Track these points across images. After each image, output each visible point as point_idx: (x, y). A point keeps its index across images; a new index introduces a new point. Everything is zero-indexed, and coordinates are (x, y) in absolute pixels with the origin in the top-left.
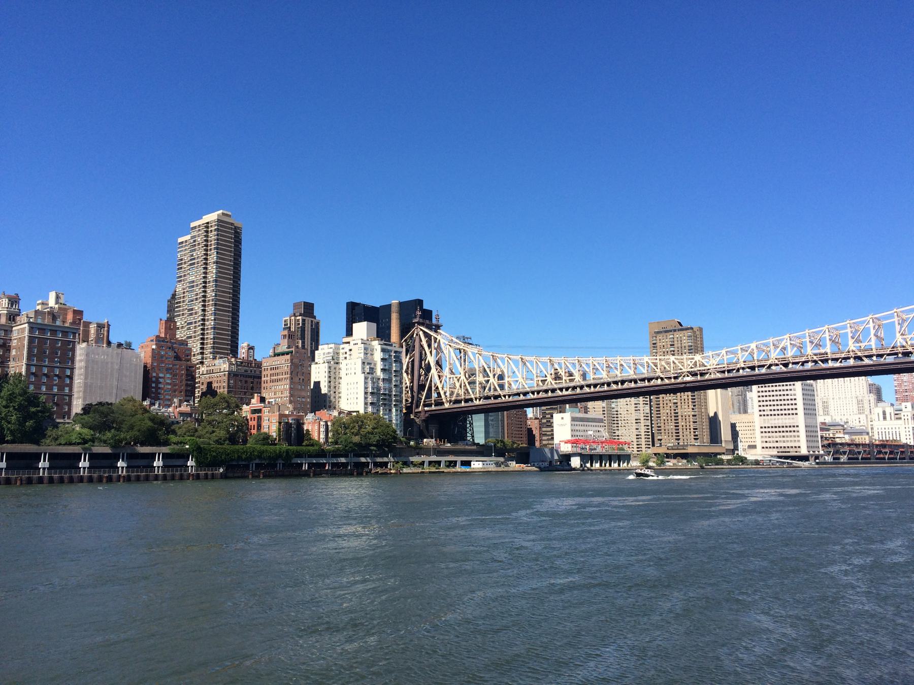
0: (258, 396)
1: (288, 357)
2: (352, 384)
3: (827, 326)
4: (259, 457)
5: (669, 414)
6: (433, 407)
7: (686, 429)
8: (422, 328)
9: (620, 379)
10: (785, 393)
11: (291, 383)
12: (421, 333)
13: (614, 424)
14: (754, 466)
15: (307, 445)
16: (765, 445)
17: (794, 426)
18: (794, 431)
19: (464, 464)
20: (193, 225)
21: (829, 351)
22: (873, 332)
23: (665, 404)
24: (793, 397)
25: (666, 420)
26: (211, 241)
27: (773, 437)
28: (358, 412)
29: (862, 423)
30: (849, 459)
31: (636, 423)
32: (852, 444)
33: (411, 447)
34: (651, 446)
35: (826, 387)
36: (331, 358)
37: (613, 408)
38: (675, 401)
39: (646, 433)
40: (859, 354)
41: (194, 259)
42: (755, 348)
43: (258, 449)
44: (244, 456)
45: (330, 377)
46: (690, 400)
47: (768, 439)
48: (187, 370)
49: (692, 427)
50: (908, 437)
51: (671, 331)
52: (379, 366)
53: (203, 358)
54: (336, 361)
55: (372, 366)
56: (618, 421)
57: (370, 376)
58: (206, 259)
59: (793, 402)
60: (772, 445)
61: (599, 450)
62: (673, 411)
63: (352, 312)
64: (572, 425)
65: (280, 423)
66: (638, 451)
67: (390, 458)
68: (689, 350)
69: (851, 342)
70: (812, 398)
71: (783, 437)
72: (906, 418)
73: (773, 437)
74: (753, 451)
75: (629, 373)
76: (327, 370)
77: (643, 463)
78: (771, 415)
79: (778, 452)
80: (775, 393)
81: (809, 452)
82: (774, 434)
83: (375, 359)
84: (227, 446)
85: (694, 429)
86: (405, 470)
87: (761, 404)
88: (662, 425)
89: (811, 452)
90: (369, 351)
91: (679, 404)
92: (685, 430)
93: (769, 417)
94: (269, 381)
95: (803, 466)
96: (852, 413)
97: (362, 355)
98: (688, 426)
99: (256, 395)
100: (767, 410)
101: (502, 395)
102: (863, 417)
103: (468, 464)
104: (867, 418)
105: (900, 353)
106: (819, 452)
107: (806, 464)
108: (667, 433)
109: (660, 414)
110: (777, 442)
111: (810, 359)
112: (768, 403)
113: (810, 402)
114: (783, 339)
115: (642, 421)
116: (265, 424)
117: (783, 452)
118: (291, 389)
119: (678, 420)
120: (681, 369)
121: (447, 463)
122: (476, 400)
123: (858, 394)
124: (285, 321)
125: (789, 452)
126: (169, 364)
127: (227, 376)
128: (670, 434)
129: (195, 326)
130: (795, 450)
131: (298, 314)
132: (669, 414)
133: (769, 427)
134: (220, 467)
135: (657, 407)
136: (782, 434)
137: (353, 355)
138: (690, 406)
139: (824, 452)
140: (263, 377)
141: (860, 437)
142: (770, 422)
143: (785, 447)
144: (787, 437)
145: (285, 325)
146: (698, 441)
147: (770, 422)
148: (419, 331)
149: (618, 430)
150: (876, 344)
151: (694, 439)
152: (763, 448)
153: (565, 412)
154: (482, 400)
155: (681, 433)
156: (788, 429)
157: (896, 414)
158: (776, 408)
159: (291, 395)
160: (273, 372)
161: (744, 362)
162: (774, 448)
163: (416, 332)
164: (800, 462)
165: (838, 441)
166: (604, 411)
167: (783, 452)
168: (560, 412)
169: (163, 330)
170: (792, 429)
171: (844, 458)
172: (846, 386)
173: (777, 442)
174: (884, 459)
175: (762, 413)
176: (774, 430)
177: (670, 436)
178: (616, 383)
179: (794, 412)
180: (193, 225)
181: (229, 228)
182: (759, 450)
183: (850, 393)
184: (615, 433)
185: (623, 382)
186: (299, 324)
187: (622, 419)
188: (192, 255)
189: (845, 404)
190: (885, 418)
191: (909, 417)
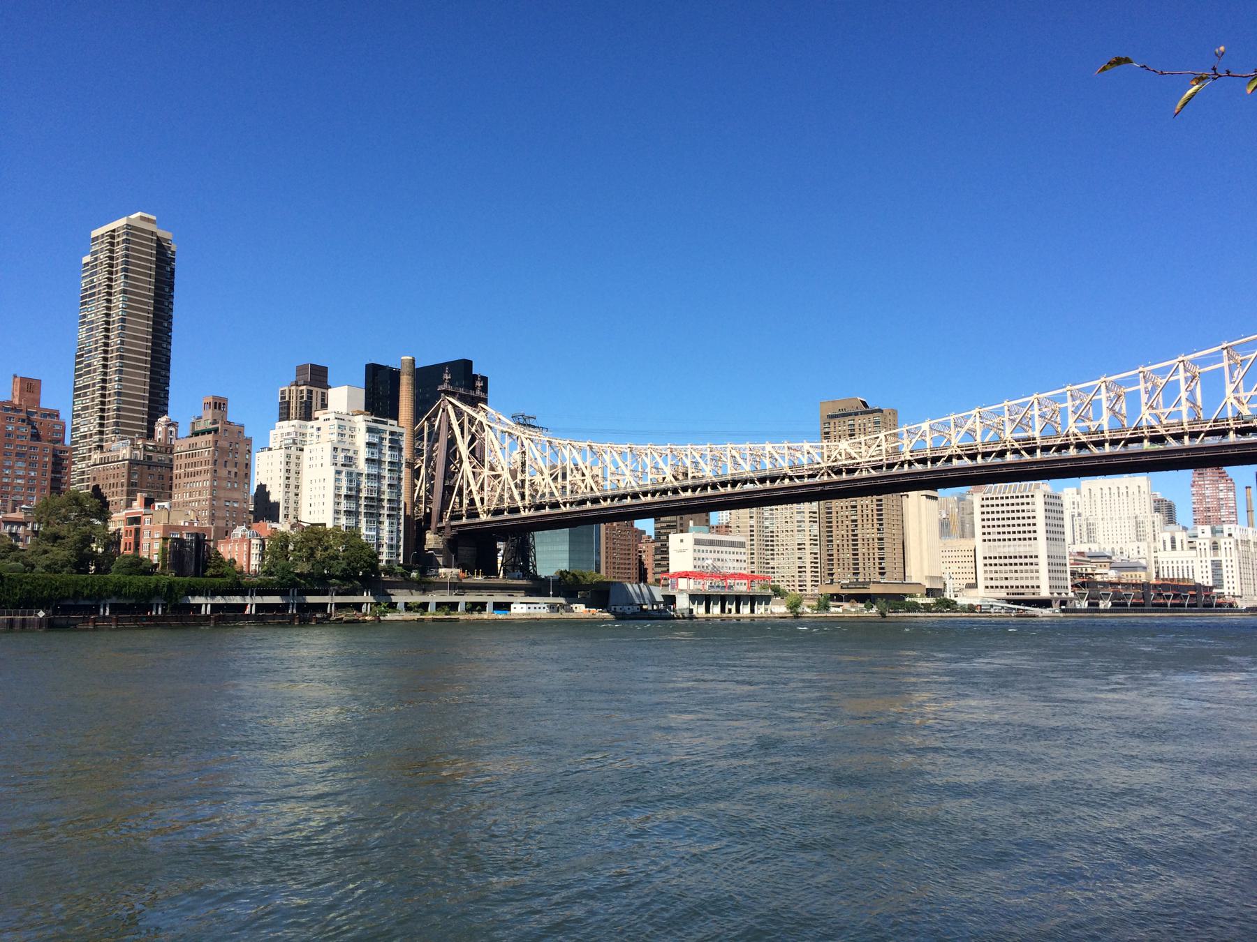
0: (142, 496)
1: (210, 437)
2: (318, 481)
3: (1035, 396)
4: (117, 593)
5: (845, 536)
6: (464, 521)
7: (869, 559)
8: (451, 399)
9: (729, 478)
10: (1020, 508)
11: (214, 479)
12: (450, 407)
13: (768, 550)
14: (964, 614)
15: (212, 576)
17: (1031, 557)
18: (1031, 564)
19: (498, 606)
20: (94, 234)
21: (1037, 434)
22: (1105, 404)
23: (840, 522)
24: (1031, 514)
25: (841, 546)
26: (118, 259)
27: (1001, 572)
28: (325, 525)
29: (1142, 554)
30: (1113, 605)
31: (799, 549)
32: (1118, 584)
33: (413, 580)
34: (819, 583)
35: (1093, 503)
36: (291, 441)
37: (767, 527)
38: (854, 518)
39: (813, 565)
40: (1084, 439)
41: (94, 287)
42: (928, 430)
43: (114, 580)
44: (86, 592)
45: (288, 471)
46: (875, 517)
47: (993, 575)
48: (55, 456)
49: (877, 555)
50: (1205, 575)
51: (850, 414)
52: (363, 453)
53: (101, 440)
54: (299, 446)
55: (351, 454)
56: (773, 546)
57: (344, 469)
58: (110, 287)
59: (1031, 521)
60: (999, 583)
61: (741, 588)
62: (850, 533)
63: (373, 379)
64: (695, 550)
65: (165, 539)
66: (800, 590)
67: (366, 598)
69: (1071, 420)
70: (1059, 515)
71: (1016, 571)
72: (1203, 547)
73: (1001, 572)
74: (972, 592)
75: (743, 468)
76: (283, 459)
77: (791, 608)
78: (999, 540)
79: (1008, 594)
80: (1005, 508)
81: (1051, 593)
82: (1003, 568)
83: (357, 444)
84: (67, 575)
85: (880, 559)
86: (389, 617)
87: (986, 523)
88: (835, 552)
89: (1056, 595)
90: (347, 432)
91: (859, 522)
92: (867, 560)
93: (997, 543)
94: (183, 475)
95: (1040, 615)
96: (1128, 540)
97: (335, 437)
98: (871, 554)
99: (139, 494)
101: (561, 501)
102: (1143, 545)
103: (506, 606)
104: (1149, 547)
105: (1146, 437)
106: (1067, 594)
107: (1047, 612)
108: (841, 565)
109: (832, 536)
110: (1007, 579)
111: (1009, 447)
112: (996, 523)
113: (1056, 522)
114: (971, 415)
115: (807, 547)
116: (145, 540)
117: (1015, 594)
118: (213, 488)
119: (857, 545)
120: (819, 463)
121: (469, 606)
122: (524, 511)
123: (1137, 512)
124: (283, 392)
125: (1023, 594)
126: (22, 446)
127: (126, 467)
128: (846, 566)
129: (94, 391)
130: (1032, 591)
131: (302, 382)
132: (845, 536)
133: (995, 558)
134: (41, 607)
135: (828, 527)
136: (1014, 568)
137: (322, 436)
138: (875, 525)
139: (1075, 594)
140: (175, 468)
141: (1133, 574)
142: (998, 550)
143: (1017, 587)
144: (1021, 571)
145: (282, 398)
146: (885, 576)
147: (998, 550)
148: (449, 406)
149: (773, 559)
150: (1110, 422)
151: (880, 573)
152: (987, 587)
153: (687, 532)
154: (532, 510)
155: (861, 565)
156: (1023, 561)
157: (1189, 542)
158: (1006, 529)
159: (214, 498)
160: (189, 460)
161: (911, 452)
163: (442, 406)
164: (1037, 609)
165: (1098, 578)
166: (752, 531)
167: (1015, 594)
168: (682, 531)
169: (17, 393)
170: (1028, 560)
171: (1105, 604)
172: (1121, 502)
173: (1007, 579)
174: (1166, 605)
175: (987, 537)
176: (1003, 561)
177: (846, 569)
178: (724, 484)
179: (1032, 535)
180: (94, 234)
181: (147, 239)
183: (1126, 512)
184: (768, 563)
185: (734, 483)
186: (302, 397)
187: (779, 543)
188: (92, 281)
189: (1118, 527)
190: (1174, 547)
191: (1207, 547)
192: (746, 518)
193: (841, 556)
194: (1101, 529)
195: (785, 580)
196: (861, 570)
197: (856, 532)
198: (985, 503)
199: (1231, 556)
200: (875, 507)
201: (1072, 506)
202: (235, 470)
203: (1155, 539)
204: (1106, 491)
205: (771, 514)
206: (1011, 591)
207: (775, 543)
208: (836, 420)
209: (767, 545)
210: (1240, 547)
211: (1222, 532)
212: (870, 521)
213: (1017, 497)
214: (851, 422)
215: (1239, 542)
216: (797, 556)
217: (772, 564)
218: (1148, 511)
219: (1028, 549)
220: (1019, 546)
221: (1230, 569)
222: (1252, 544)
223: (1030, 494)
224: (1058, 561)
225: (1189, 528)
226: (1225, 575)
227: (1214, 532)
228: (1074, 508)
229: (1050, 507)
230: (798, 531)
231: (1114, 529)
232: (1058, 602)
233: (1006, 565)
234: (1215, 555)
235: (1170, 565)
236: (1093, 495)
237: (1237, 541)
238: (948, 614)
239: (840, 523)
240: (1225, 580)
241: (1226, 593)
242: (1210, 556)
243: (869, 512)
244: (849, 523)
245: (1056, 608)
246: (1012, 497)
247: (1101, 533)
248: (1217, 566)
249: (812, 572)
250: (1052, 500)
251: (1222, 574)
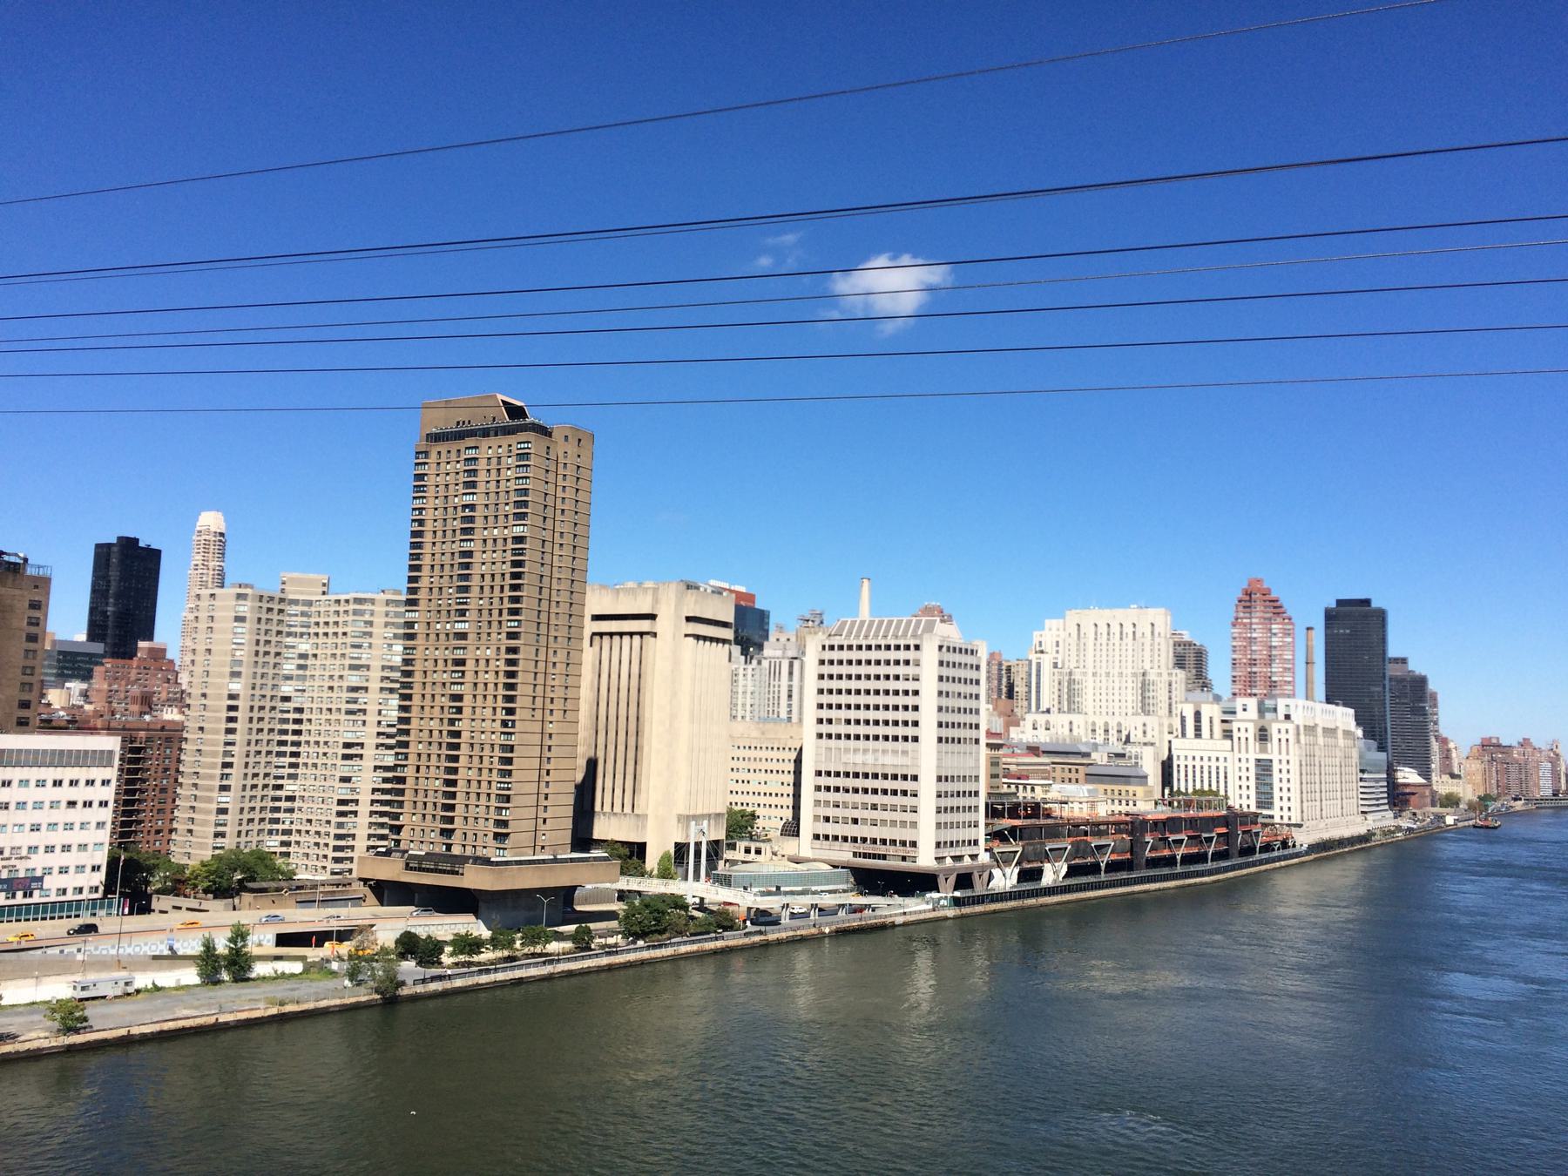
5: (436, 733)
13: (283, 754)
16: (825, 829)
17: (905, 777)
18: (905, 793)
23: (428, 697)
24: (911, 686)
25: (424, 757)
29: (1149, 738)
30: (1073, 871)
31: (346, 757)
35: (1082, 645)
37: (286, 699)
38: (456, 689)
47: (831, 812)
49: (494, 790)
56: (298, 744)
59: (910, 700)
62: (446, 728)
66: (337, 860)
68: (518, 504)
71: (874, 807)
72: (1243, 735)
73: (846, 806)
78: (848, 737)
79: (855, 854)
82: (850, 797)
91: (467, 701)
93: (843, 743)
96: (1130, 711)
98: (485, 784)
100: (839, 720)
104: (1161, 725)
109: (407, 732)
110: (855, 821)
115: (369, 752)
123: (1147, 666)
125: (884, 857)
130: (901, 851)
132: (436, 733)
133: (838, 774)
136: (870, 799)
138: (499, 710)
139: (993, 856)
141: (1123, 788)
143: (874, 841)
146: (508, 843)
149: (293, 777)
151: (497, 836)
152: (817, 837)
155: (460, 810)
157: (1223, 721)
162: (845, 839)
170: (899, 785)
171: (1053, 874)
172: (1124, 648)
173: (855, 821)
174: (1174, 857)
175: (825, 729)
176: (851, 783)
182: (804, 845)
183: (1130, 663)
184: (280, 787)
189: (1117, 688)
190: (1198, 735)
192: (221, 675)
193: (422, 783)
194: (1090, 691)
195: (313, 829)
196: (458, 823)
197: (458, 727)
198: (828, 655)
199: (1288, 753)
200: (503, 667)
201: (1055, 649)
203: (1170, 712)
204: (1103, 629)
205: (300, 667)
206: (862, 848)
207: (302, 738)
208: (443, 447)
209: (282, 743)
210: (1302, 737)
211: (1275, 710)
212: (490, 698)
213: (888, 647)
214: (471, 453)
215: (1302, 729)
216: (338, 775)
217: (290, 787)
218: (1163, 662)
219: (900, 760)
220: (884, 752)
221: (1285, 776)
222: (1320, 731)
223: (912, 643)
224: (961, 787)
225: (1225, 698)
226: (1276, 785)
227: (1262, 710)
228: (1057, 652)
229: (951, 672)
230: (349, 712)
231: (1111, 691)
232: (952, 879)
233: (856, 791)
234: (1264, 750)
235: (1190, 763)
236: (1082, 635)
237: (1298, 727)
238: (646, 955)
239: (428, 701)
240: (1277, 794)
241: (1277, 820)
242: (1253, 753)
243: (490, 677)
244: (445, 701)
245: (946, 892)
246: (879, 647)
247: (1090, 697)
248: (1264, 768)
249: (372, 813)
250: (957, 658)
251: (1271, 784)
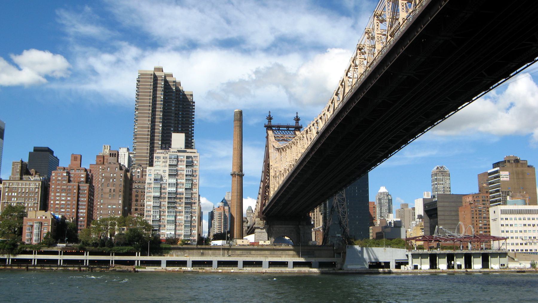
202: (114, 188)
